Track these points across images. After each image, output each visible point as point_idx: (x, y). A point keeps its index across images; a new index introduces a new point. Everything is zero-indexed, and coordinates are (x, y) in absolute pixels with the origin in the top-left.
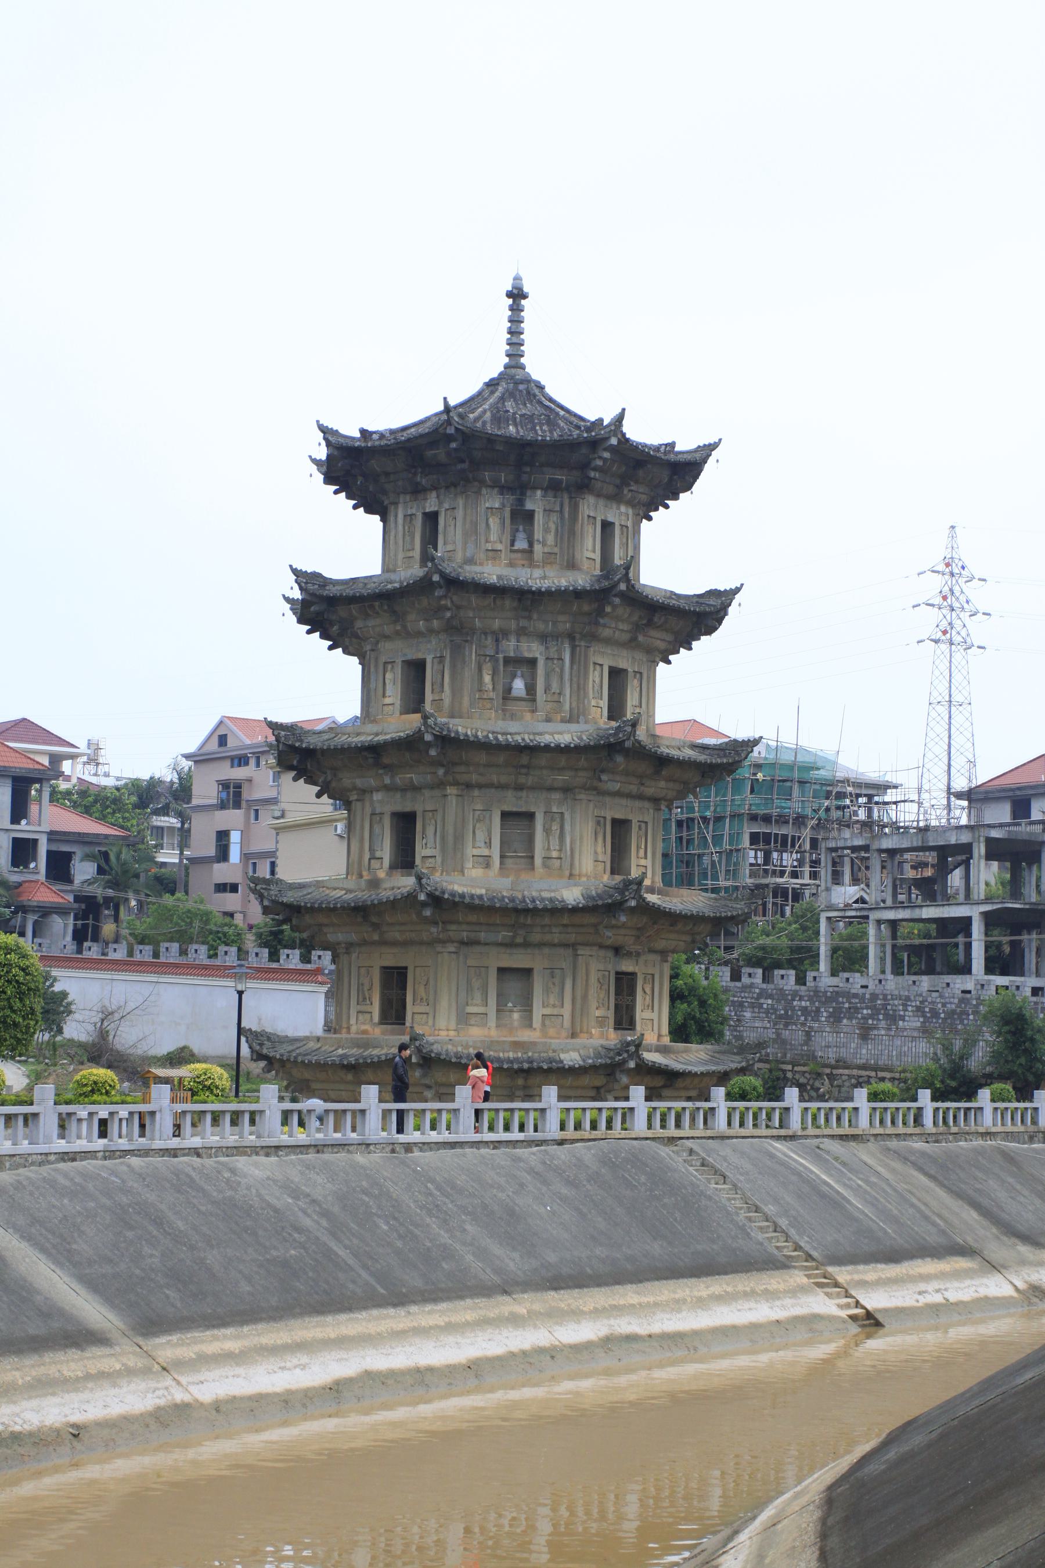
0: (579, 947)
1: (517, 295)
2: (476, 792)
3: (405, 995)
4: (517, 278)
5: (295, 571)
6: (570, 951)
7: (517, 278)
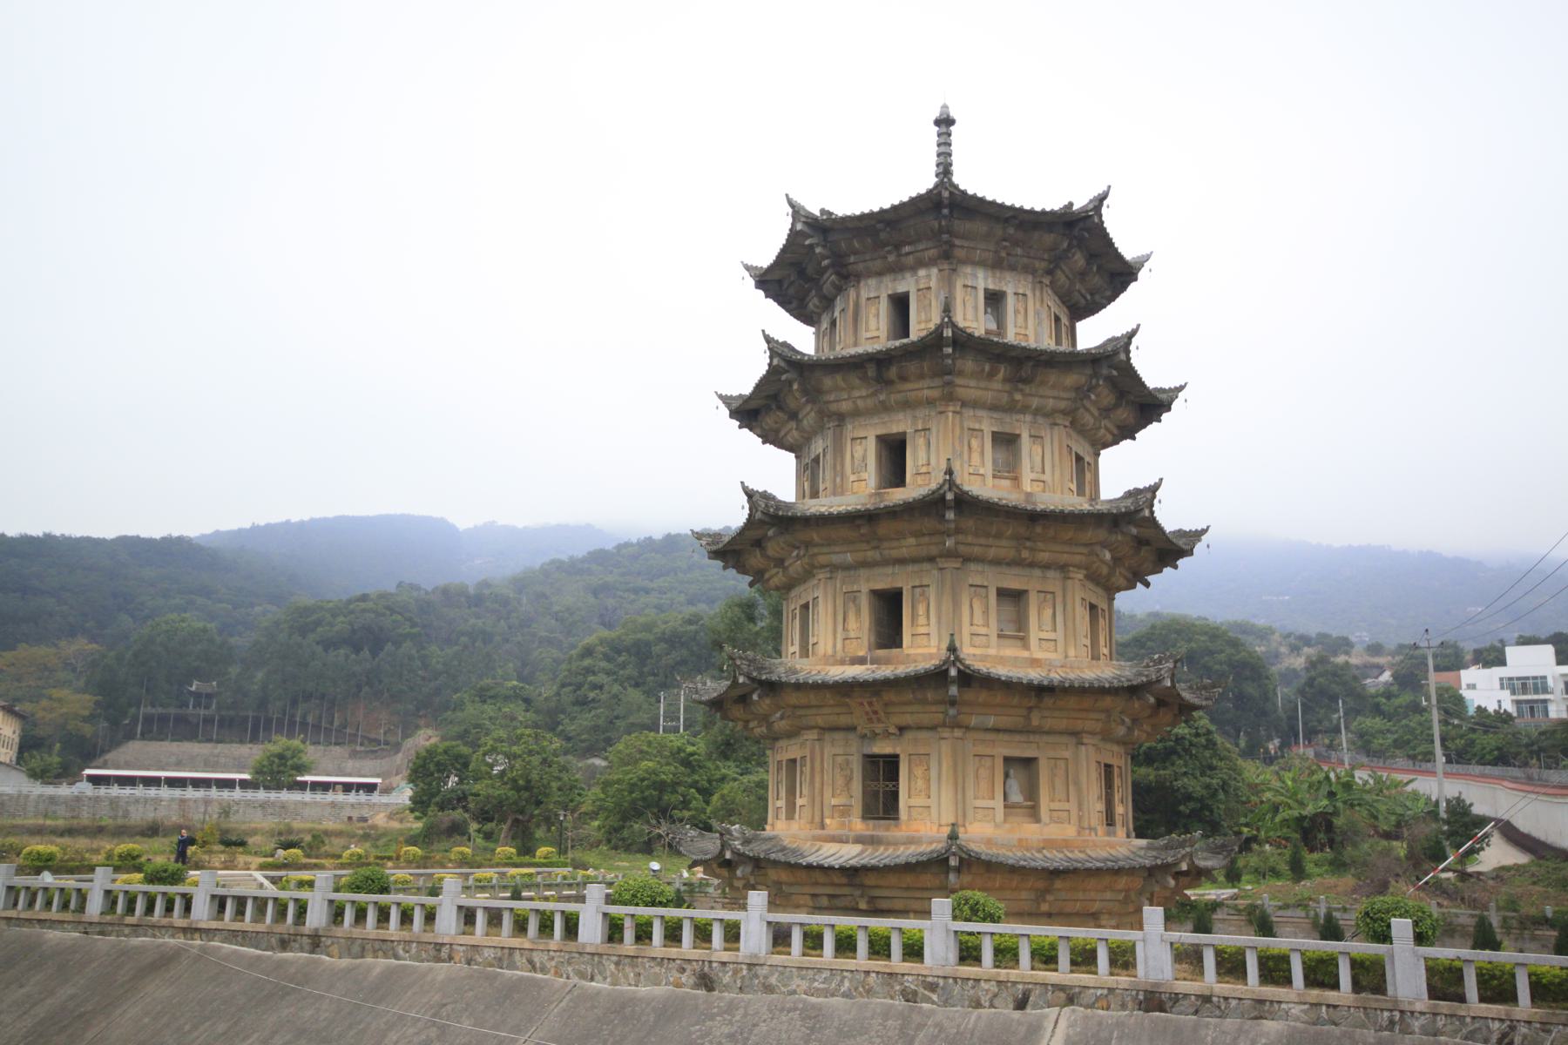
0: (1084, 735)
1: (945, 122)
2: (973, 566)
3: (897, 786)
4: (945, 107)
5: (768, 339)
6: (1073, 740)
7: (945, 107)
